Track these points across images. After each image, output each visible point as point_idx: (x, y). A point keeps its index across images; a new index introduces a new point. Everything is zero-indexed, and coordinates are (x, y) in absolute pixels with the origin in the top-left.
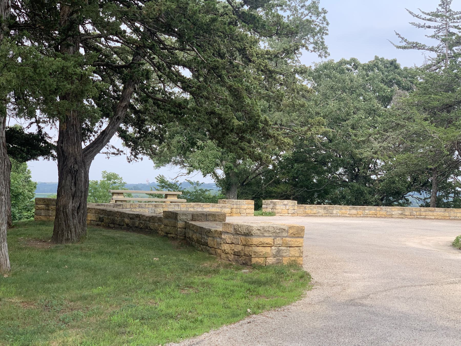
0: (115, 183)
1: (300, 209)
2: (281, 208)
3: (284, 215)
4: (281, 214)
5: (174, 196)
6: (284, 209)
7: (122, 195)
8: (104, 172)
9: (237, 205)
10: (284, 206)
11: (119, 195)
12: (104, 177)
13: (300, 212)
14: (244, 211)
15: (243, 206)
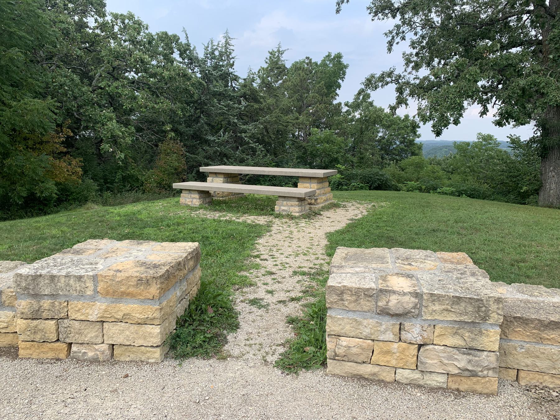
0: (490, 144)
1: (541, 341)
2: (366, 332)
3: (388, 376)
4: (366, 370)
5: (313, 181)
6: (389, 336)
7: (220, 176)
8: (479, 134)
9: (36, 296)
10: (388, 323)
11: (217, 177)
12: (479, 139)
13: (542, 364)
14: (91, 334)
15: (75, 304)
